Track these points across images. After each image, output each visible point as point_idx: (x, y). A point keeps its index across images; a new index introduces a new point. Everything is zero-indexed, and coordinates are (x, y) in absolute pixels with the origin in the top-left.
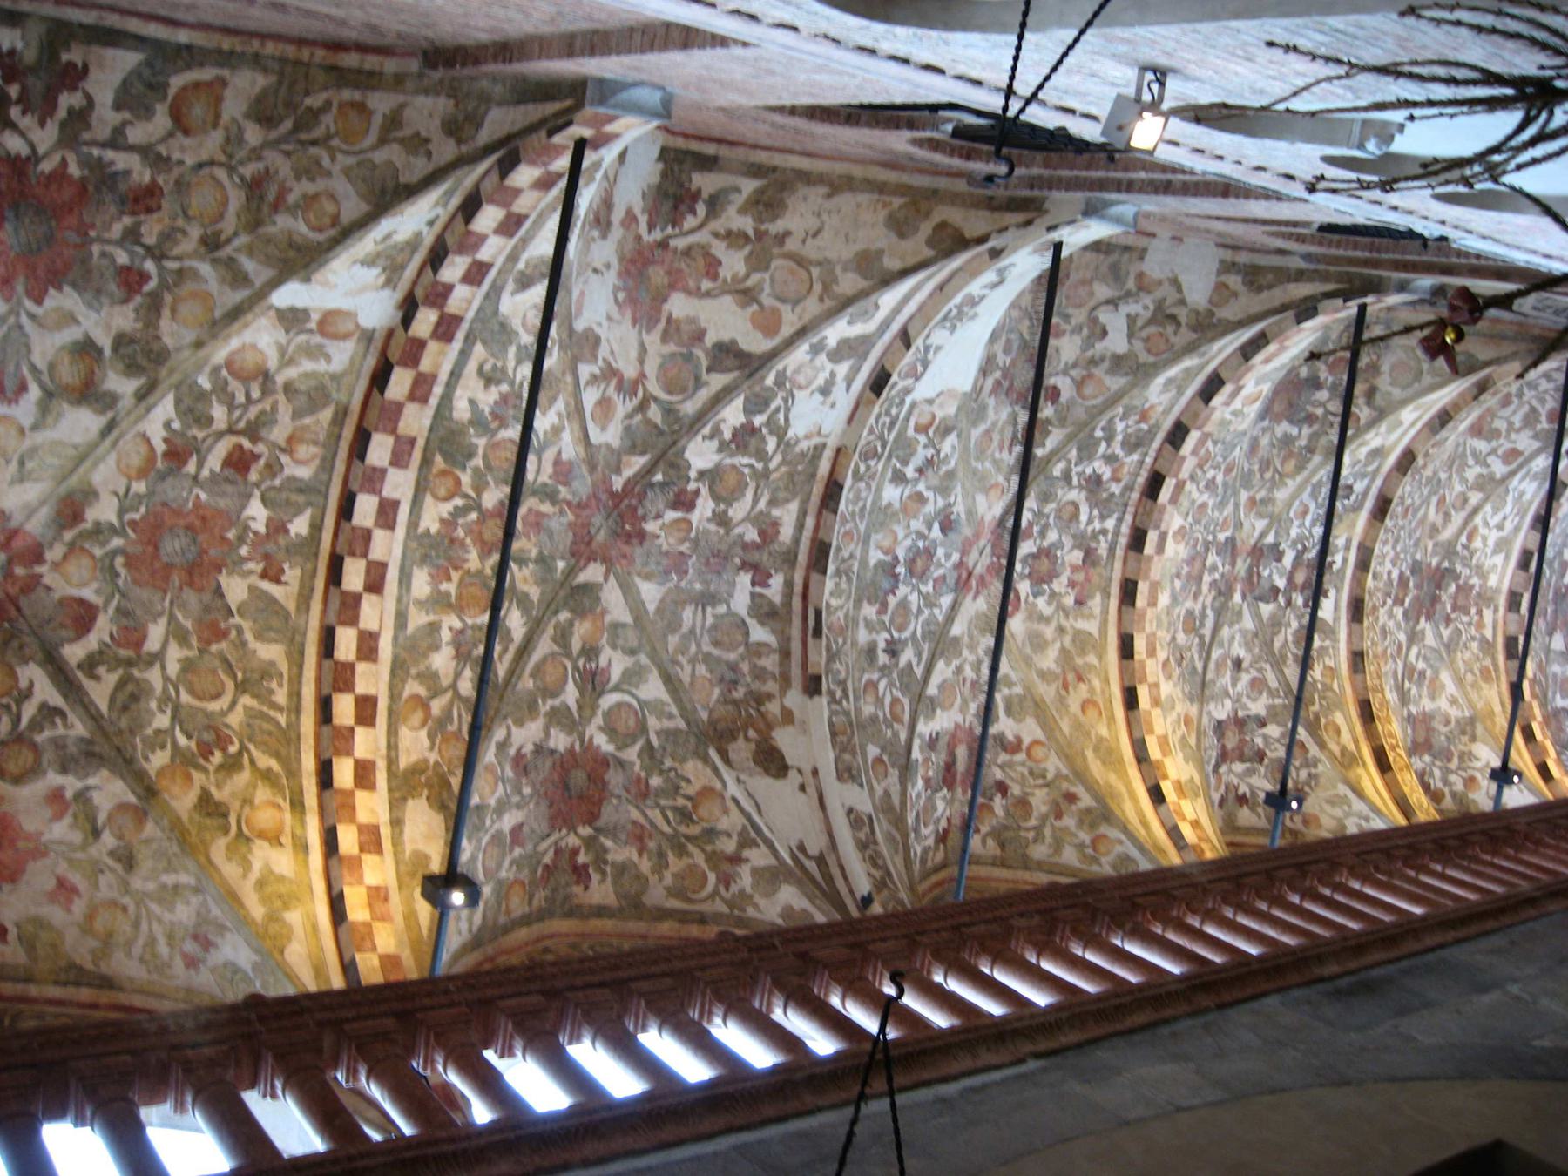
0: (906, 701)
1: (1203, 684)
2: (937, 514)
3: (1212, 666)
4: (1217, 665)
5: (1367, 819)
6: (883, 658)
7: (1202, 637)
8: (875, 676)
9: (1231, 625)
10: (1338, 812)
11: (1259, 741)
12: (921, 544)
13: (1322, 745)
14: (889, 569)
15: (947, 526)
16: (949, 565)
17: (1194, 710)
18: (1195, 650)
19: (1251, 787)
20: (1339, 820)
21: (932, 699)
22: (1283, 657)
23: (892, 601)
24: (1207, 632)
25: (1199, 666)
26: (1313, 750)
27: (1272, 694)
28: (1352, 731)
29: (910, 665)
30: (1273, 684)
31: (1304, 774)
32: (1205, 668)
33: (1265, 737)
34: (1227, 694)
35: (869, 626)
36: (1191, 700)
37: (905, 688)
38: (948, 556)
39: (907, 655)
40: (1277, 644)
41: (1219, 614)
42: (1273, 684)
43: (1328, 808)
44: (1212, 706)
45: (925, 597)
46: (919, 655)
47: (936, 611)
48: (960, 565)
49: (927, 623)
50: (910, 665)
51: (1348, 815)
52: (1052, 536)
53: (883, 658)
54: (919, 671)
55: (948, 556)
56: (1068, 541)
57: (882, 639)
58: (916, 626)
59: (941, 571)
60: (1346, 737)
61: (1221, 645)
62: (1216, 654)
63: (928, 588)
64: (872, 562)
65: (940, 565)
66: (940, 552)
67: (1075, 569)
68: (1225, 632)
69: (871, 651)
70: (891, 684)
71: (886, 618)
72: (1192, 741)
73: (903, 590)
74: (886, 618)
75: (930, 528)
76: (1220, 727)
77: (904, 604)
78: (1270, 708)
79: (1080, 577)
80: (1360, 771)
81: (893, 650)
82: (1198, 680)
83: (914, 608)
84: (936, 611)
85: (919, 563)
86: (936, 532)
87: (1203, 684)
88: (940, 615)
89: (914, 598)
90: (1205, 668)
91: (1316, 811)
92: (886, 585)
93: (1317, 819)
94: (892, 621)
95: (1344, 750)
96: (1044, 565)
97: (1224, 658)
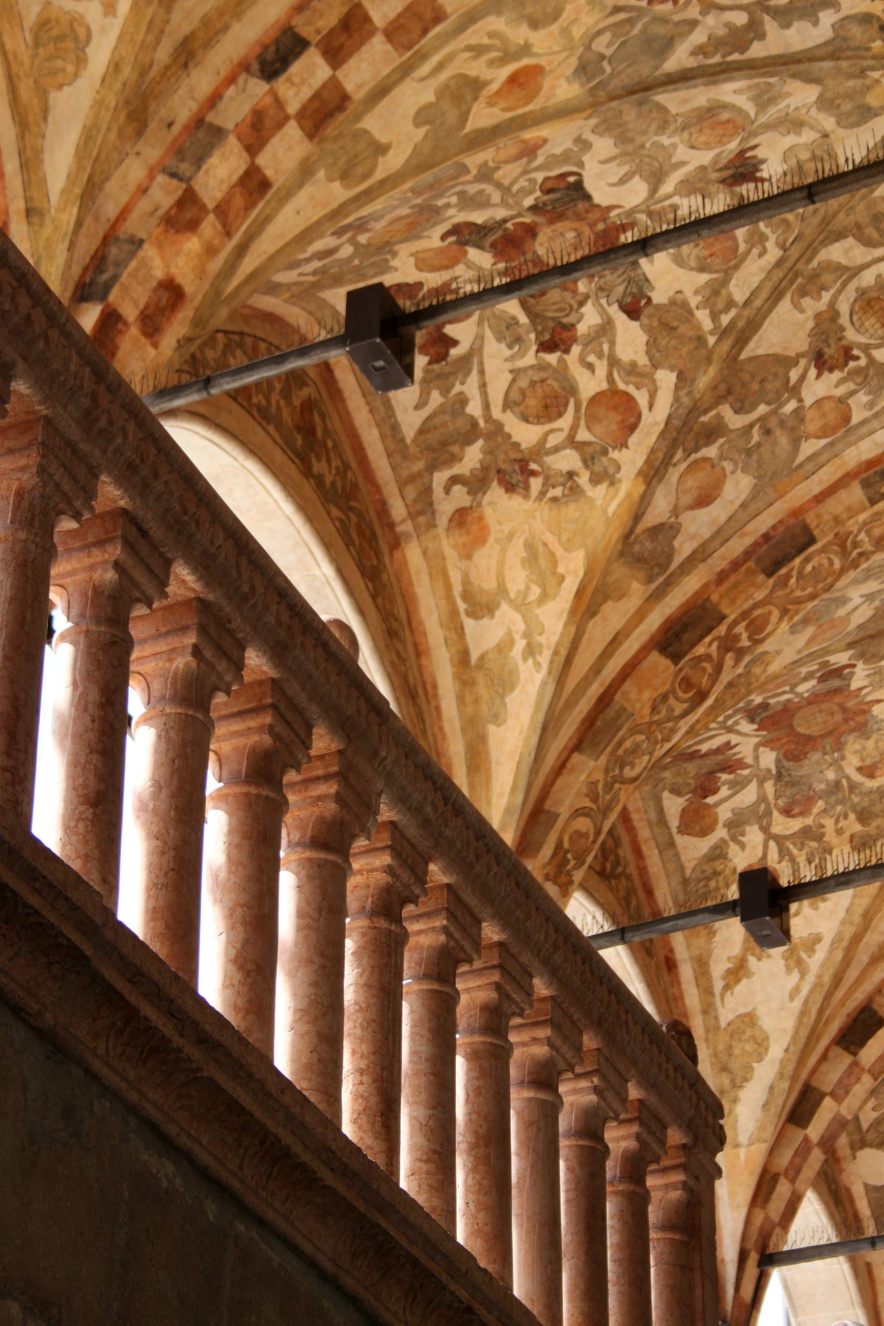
1: (643, 89)
3: (700, 96)
4: (712, 110)
5: (531, 651)
7: (754, 30)
9: (825, 103)
10: (517, 579)
11: (589, 318)
13: (653, 473)
17: (563, 89)
18: (712, 24)
19: (477, 350)
20: (502, 589)
22: (812, 285)
24: (779, 39)
25: (680, 58)
26: (631, 458)
27: (714, 293)
28: (721, 535)
30: (740, 287)
31: (567, 461)
32: (683, 77)
33: (606, 328)
34: (656, 179)
36: (584, 70)
40: (837, 252)
41: (834, 50)
42: (740, 287)
43: (517, 551)
44: (604, 146)
51: (521, 605)
60: (699, 524)
61: (764, 100)
62: (733, 92)
68: (801, 96)
72: (483, 116)
76: (567, 195)
78: (679, 306)
80: (637, 591)
82: (644, 70)
87: (643, 89)
90: (683, 77)
91: (496, 530)
93: (481, 539)
95: (665, 531)
97: (738, 124)
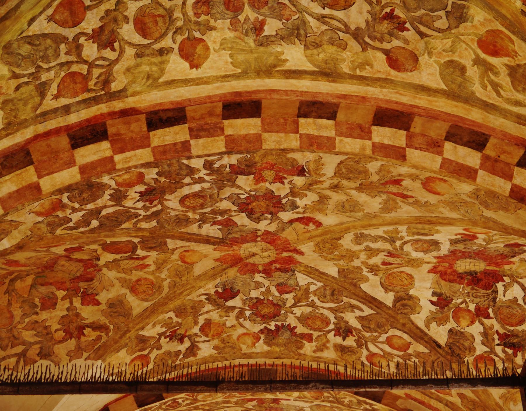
0: (392, 332)
2: (218, 306)
6: (350, 341)
8: (365, 352)
12: (248, 313)
14: (271, 335)
15: (229, 293)
16: (267, 283)
21: (397, 300)
23: (301, 329)
29: (361, 319)
35: (320, 349)
37: (380, 328)
38: (258, 285)
39: (351, 319)
45: (297, 302)
46: (353, 307)
47: (312, 288)
48: (267, 272)
49: (323, 297)
50: (361, 319)
52: (225, 205)
53: (350, 341)
54: (368, 311)
55: (258, 285)
56: (228, 192)
57: (334, 339)
58: (325, 309)
59: (273, 289)
63: (289, 298)
64: (266, 348)
65: (268, 291)
66: (254, 294)
67: (260, 179)
69: (342, 349)
70: (375, 341)
71: (315, 334)
73: (292, 321)
74: (315, 334)
75: (233, 308)
77: (303, 320)
79: (269, 174)
81: (345, 331)
83: (309, 309)
84: (312, 288)
85: (265, 311)
86: (236, 302)
88: (316, 285)
89: (298, 311)
92: (287, 334)
94: (319, 330)
96: (258, 205)
